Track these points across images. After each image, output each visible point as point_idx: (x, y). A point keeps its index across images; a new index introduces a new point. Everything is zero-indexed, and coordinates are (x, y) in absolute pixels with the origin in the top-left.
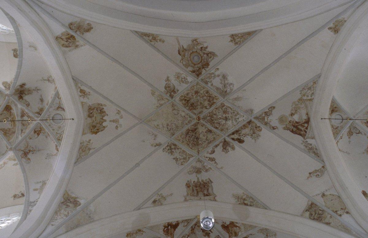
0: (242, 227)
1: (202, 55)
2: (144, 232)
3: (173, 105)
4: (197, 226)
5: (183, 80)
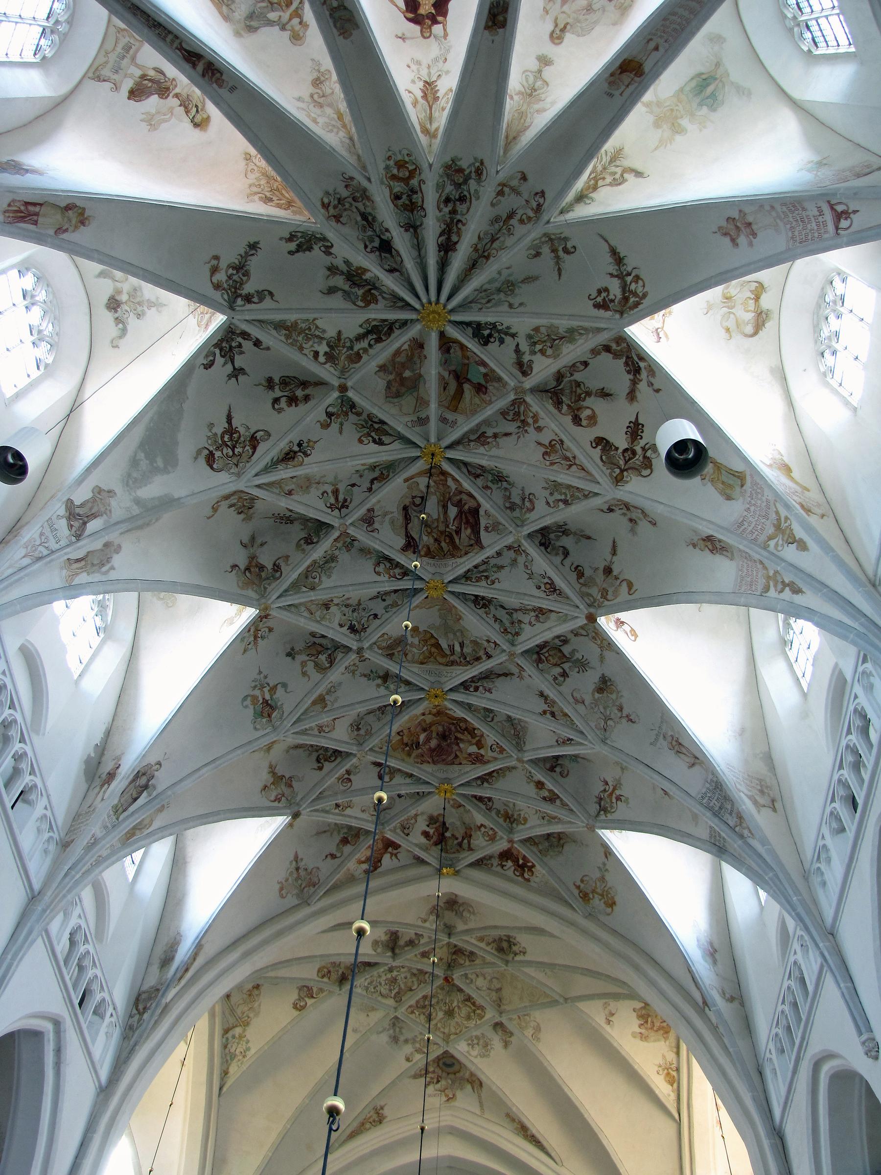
1: (436, 1070)
3: (499, 1003)
4: (457, 839)
5: (475, 1041)
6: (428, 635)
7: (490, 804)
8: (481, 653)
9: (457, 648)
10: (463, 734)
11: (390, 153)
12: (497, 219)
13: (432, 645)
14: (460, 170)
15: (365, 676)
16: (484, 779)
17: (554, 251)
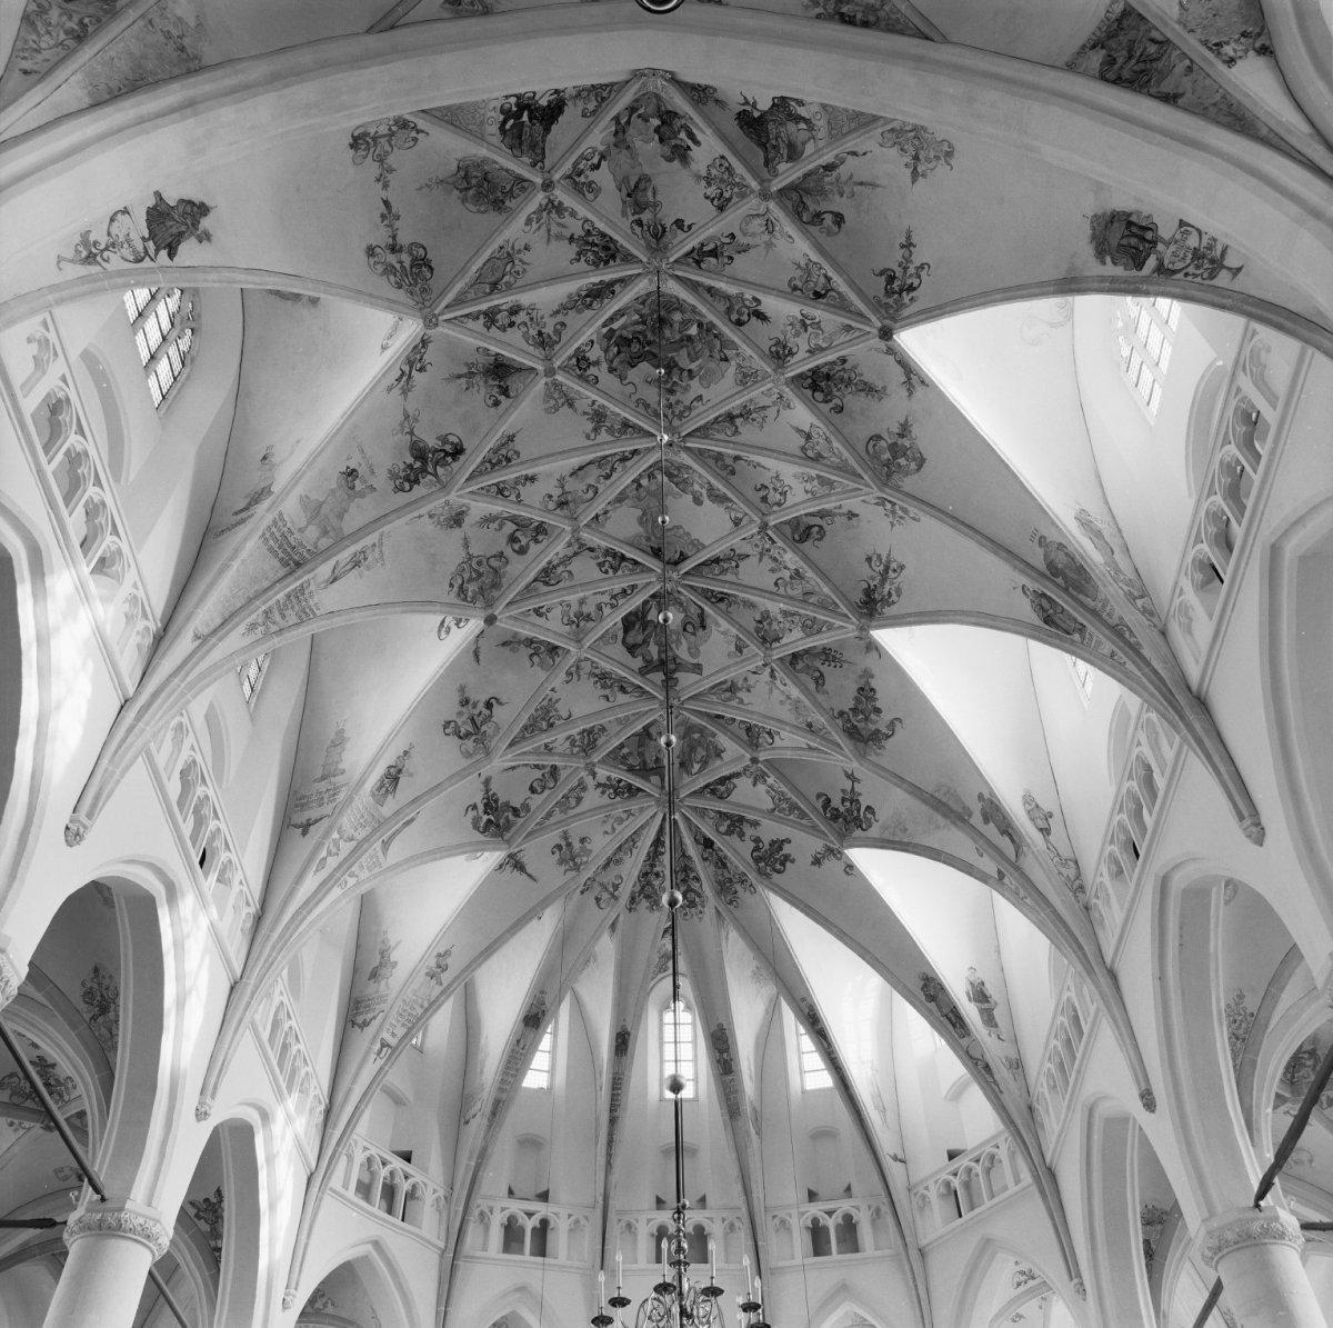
0: (821, 123)
2: (422, 131)
4: (639, 116)
7: (586, 227)
10: (635, 332)
11: (700, 916)
12: (618, 862)
14: (647, 897)
16: (599, 293)
17: (569, 845)
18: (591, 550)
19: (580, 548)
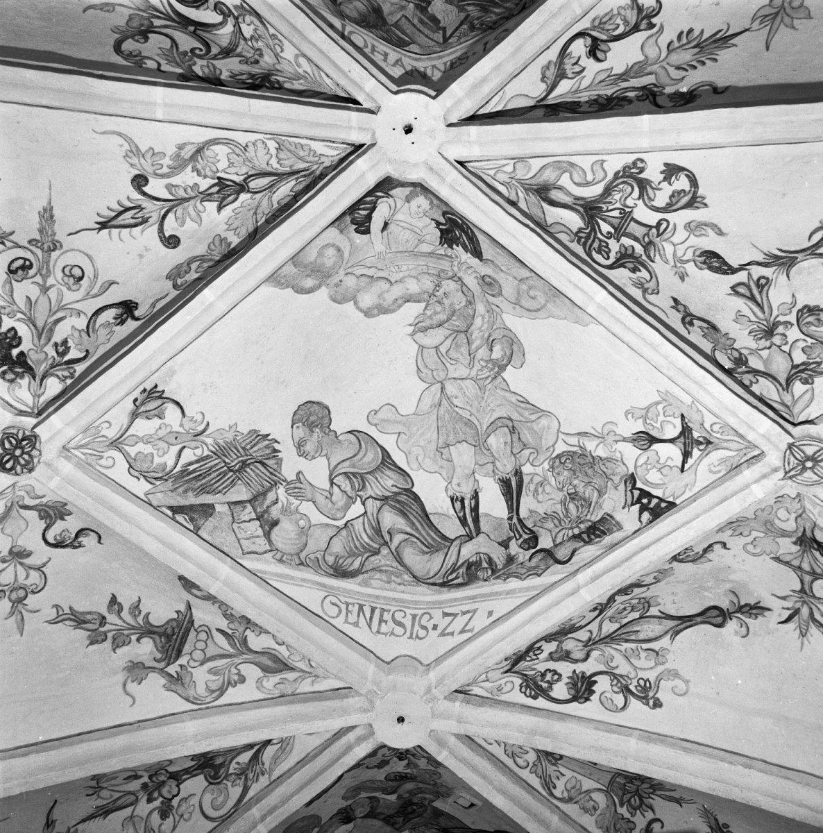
6: (371, 458)
8: (614, 502)
9: (493, 504)
13: (385, 499)
15: (78, 620)
18: (713, 261)
19: (763, 284)
